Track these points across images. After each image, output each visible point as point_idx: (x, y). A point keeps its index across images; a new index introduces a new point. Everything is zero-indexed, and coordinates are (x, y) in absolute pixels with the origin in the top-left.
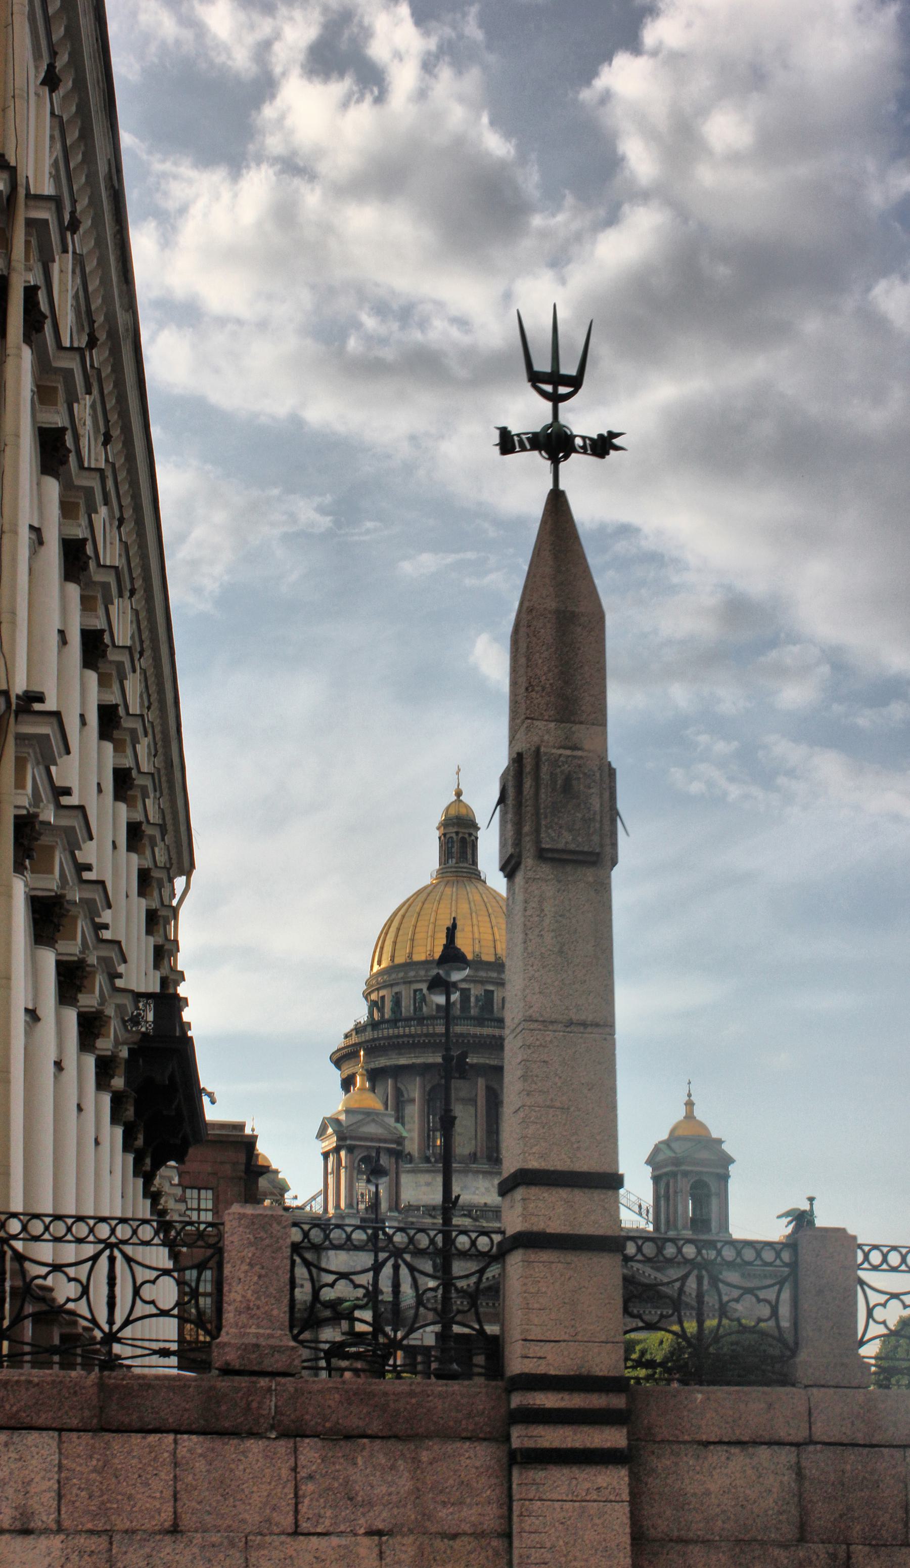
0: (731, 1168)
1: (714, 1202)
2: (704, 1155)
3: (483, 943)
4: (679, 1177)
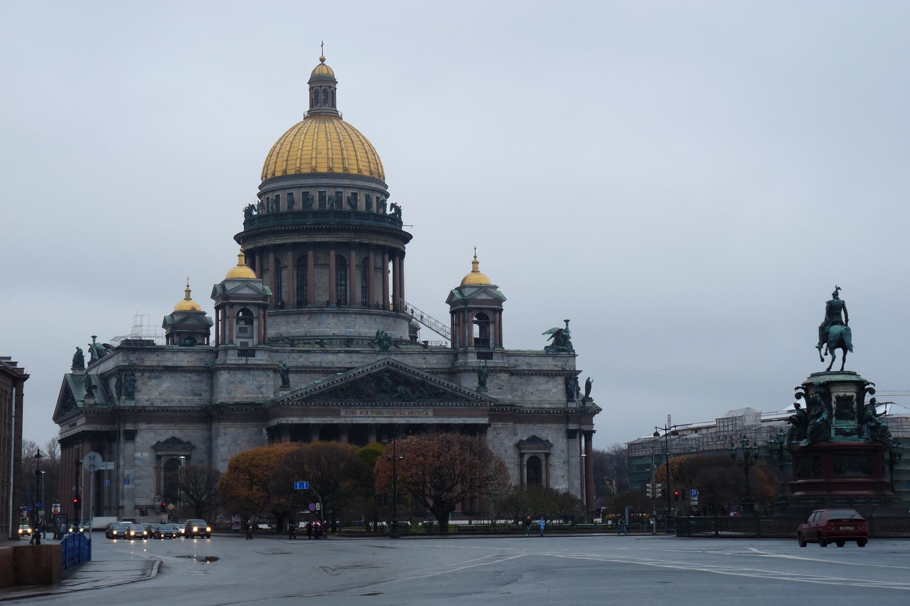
0: (503, 304)
2: (484, 297)
3: (335, 161)
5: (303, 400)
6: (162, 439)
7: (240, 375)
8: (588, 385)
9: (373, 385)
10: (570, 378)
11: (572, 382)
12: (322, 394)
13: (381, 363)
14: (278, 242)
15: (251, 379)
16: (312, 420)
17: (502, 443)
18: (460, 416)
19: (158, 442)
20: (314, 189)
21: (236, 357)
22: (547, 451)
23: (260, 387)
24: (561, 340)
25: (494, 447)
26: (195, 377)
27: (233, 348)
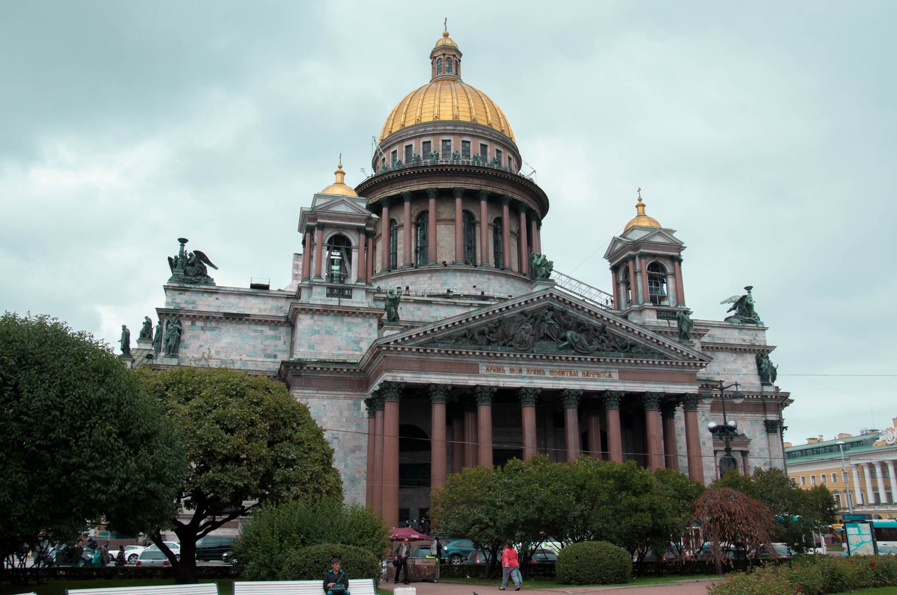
2: (659, 239)
4: (637, 259)
5: (421, 345)
7: (328, 322)
9: (529, 326)
10: (762, 356)
11: (764, 360)
12: (450, 337)
13: (541, 295)
14: (393, 193)
15: (346, 328)
18: (658, 381)
22: (744, 449)
23: (357, 342)
24: (744, 308)
26: (267, 331)
27: (320, 285)
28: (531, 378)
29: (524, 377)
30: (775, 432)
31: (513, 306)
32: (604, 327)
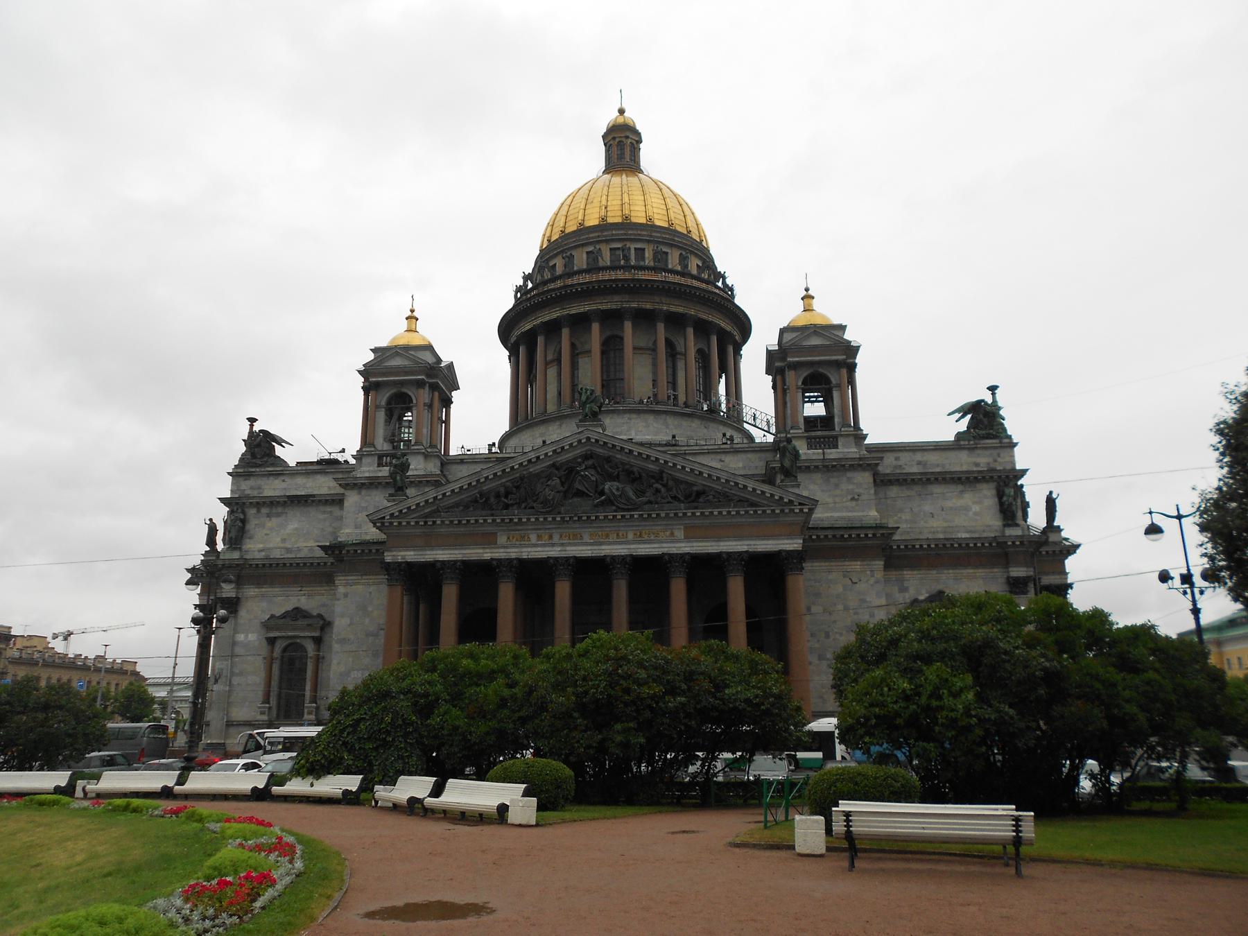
1: (836, 394)
5: (427, 516)
6: (279, 611)
8: (1051, 504)
10: (1006, 485)
12: (457, 505)
14: (528, 327)
16: (442, 555)
17: (863, 601)
18: (740, 538)
19: (273, 616)
20: (580, 250)
21: (375, 467)
24: (984, 420)
25: (846, 609)
27: (369, 455)
28: (562, 545)
29: (553, 545)
30: (1025, 593)
31: (538, 458)
32: (662, 472)
